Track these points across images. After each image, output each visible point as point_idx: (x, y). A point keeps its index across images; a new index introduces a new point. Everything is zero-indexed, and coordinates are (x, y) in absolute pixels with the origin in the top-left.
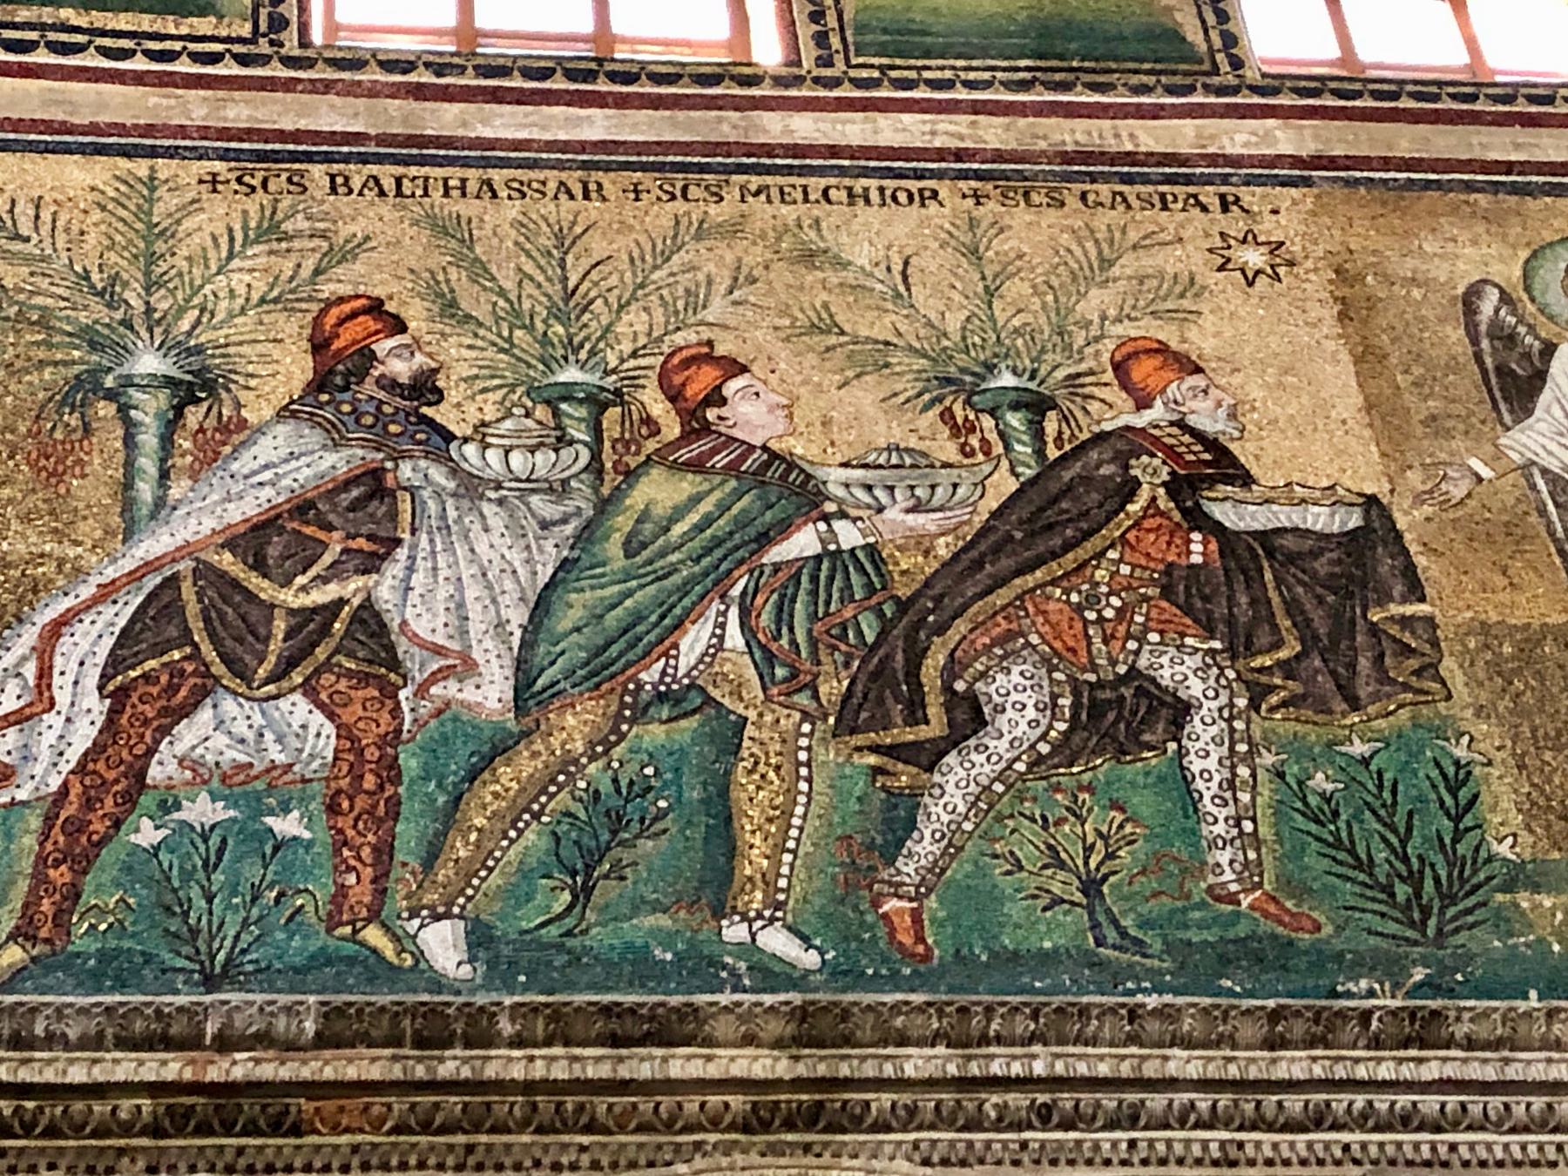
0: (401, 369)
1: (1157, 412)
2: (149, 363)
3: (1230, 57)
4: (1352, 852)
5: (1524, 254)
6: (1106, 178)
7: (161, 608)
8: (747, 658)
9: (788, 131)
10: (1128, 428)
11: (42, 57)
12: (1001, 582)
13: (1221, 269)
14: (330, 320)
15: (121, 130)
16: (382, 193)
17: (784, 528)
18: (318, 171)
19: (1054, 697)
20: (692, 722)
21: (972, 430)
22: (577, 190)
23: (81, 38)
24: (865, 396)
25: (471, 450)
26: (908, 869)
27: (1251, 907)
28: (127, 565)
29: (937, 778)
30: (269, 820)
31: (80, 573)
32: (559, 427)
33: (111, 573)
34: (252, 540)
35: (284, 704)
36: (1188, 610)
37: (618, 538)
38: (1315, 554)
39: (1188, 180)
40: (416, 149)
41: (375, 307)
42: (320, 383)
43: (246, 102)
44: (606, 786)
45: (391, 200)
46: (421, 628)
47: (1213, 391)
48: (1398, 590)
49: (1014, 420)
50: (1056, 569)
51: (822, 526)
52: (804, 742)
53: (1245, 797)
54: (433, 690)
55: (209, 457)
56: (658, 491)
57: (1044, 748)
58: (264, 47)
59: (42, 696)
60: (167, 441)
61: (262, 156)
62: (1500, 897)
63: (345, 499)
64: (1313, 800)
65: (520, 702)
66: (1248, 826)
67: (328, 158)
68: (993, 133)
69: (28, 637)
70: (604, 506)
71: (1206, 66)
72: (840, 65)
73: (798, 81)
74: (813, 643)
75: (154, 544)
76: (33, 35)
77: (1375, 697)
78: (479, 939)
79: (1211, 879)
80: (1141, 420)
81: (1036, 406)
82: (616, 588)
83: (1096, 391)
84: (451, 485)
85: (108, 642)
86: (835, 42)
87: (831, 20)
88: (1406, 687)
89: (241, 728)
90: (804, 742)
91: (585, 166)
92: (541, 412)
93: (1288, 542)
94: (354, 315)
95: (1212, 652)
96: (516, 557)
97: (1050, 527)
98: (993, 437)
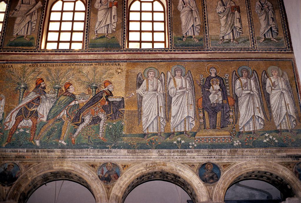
0: (43, 86)
1: (106, 89)
2: (23, 86)
3: (123, 47)
4: (111, 134)
5: (144, 69)
6: (108, 62)
7: (20, 111)
8: (66, 115)
9: (81, 57)
10: (103, 90)
11: (18, 52)
12: (89, 107)
13: (116, 72)
14: (38, 81)
15: (23, 60)
16: (44, 66)
17: (72, 102)
18: (39, 64)
19: (90, 119)
20: (60, 122)
21: (90, 91)
22: (61, 65)
23: (21, 50)
24: (81, 87)
25: (47, 94)
26: (75, 136)
27: (102, 139)
28: (18, 107)
29: (79, 127)
30: (26, 131)
31: (15, 108)
32: (55, 92)
33: (17, 108)
34: (28, 104)
35: (29, 120)
36: (104, 110)
37: (58, 103)
38: (116, 104)
39: (116, 62)
40: (47, 61)
41: (42, 79)
42: (36, 88)
43: (34, 56)
44: (52, 128)
45: (45, 67)
46: (40, 113)
47: (112, 86)
48: (122, 107)
49: (94, 90)
50: (94, 105)
51: (75, 102)
52: (69, 123)
53: (104, 128)
54: (40, 119)
55: (26, 96)
56: (62, 98)
57: (88, 124)
58: (37, 50)
59: (11, 120)
60: (23, 94)
61: (35, 63)
62: (122, 138)
63: (36, 100)
64: (109, 129)
65: (47, 120)
66: (103, 131)
67: (40, 63)
68: (99, 57)
69: (10, 114)
70: (57, 100)
71: (121, 48)
72: (87, 49)
73: (83, 51)
74: (72, 114)
75: (21, 105)
76: (17, 50)
77: (117, 118)
78: (40, 142)
79: (99, 136)
80: (104, 90)
81: (96, 88)
82: (57, 108)
83: (102, 86)
84: (45, 98)
85: (16, 114)
86: (87, 46)
87: (87, 44)
88: (120, 117)
89: (25, 123)
90: (69, 123)
91: (62, 62)
92: (54, 90)
93: (114, 102)
94: (40, 80)
95: (105, 114)
96: (49, 105)
97: (94, 101)
98: (92, 91)
